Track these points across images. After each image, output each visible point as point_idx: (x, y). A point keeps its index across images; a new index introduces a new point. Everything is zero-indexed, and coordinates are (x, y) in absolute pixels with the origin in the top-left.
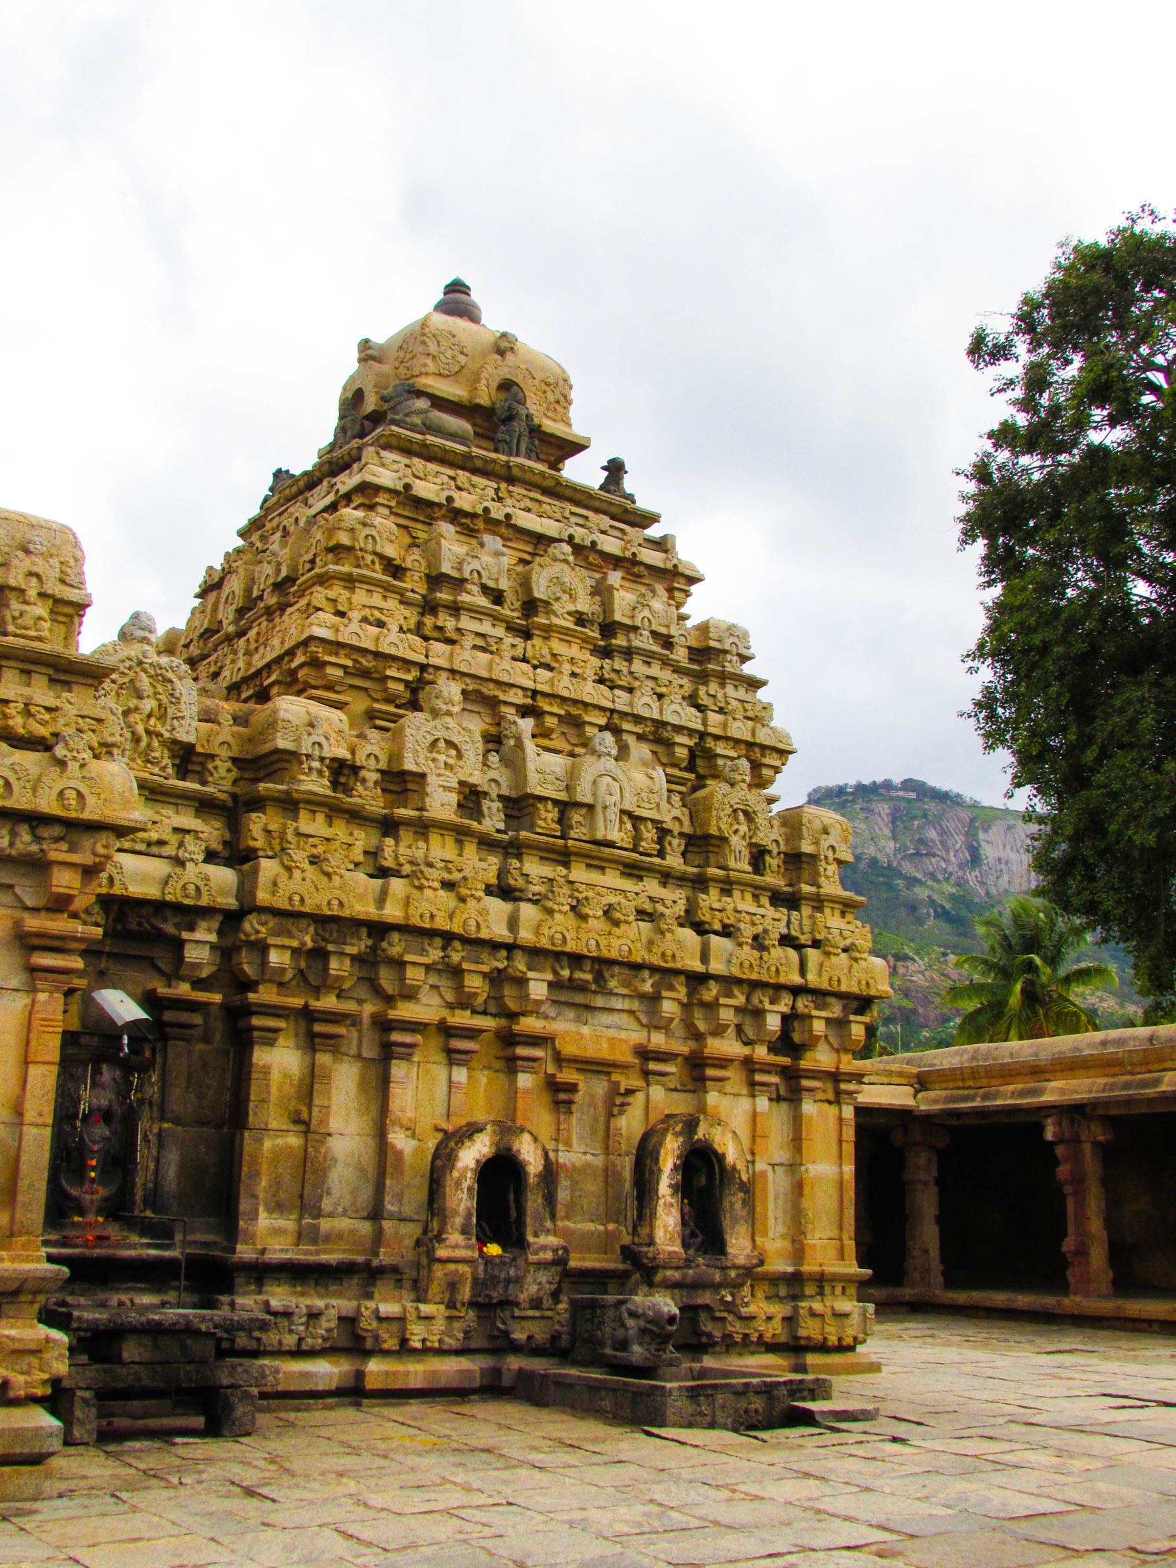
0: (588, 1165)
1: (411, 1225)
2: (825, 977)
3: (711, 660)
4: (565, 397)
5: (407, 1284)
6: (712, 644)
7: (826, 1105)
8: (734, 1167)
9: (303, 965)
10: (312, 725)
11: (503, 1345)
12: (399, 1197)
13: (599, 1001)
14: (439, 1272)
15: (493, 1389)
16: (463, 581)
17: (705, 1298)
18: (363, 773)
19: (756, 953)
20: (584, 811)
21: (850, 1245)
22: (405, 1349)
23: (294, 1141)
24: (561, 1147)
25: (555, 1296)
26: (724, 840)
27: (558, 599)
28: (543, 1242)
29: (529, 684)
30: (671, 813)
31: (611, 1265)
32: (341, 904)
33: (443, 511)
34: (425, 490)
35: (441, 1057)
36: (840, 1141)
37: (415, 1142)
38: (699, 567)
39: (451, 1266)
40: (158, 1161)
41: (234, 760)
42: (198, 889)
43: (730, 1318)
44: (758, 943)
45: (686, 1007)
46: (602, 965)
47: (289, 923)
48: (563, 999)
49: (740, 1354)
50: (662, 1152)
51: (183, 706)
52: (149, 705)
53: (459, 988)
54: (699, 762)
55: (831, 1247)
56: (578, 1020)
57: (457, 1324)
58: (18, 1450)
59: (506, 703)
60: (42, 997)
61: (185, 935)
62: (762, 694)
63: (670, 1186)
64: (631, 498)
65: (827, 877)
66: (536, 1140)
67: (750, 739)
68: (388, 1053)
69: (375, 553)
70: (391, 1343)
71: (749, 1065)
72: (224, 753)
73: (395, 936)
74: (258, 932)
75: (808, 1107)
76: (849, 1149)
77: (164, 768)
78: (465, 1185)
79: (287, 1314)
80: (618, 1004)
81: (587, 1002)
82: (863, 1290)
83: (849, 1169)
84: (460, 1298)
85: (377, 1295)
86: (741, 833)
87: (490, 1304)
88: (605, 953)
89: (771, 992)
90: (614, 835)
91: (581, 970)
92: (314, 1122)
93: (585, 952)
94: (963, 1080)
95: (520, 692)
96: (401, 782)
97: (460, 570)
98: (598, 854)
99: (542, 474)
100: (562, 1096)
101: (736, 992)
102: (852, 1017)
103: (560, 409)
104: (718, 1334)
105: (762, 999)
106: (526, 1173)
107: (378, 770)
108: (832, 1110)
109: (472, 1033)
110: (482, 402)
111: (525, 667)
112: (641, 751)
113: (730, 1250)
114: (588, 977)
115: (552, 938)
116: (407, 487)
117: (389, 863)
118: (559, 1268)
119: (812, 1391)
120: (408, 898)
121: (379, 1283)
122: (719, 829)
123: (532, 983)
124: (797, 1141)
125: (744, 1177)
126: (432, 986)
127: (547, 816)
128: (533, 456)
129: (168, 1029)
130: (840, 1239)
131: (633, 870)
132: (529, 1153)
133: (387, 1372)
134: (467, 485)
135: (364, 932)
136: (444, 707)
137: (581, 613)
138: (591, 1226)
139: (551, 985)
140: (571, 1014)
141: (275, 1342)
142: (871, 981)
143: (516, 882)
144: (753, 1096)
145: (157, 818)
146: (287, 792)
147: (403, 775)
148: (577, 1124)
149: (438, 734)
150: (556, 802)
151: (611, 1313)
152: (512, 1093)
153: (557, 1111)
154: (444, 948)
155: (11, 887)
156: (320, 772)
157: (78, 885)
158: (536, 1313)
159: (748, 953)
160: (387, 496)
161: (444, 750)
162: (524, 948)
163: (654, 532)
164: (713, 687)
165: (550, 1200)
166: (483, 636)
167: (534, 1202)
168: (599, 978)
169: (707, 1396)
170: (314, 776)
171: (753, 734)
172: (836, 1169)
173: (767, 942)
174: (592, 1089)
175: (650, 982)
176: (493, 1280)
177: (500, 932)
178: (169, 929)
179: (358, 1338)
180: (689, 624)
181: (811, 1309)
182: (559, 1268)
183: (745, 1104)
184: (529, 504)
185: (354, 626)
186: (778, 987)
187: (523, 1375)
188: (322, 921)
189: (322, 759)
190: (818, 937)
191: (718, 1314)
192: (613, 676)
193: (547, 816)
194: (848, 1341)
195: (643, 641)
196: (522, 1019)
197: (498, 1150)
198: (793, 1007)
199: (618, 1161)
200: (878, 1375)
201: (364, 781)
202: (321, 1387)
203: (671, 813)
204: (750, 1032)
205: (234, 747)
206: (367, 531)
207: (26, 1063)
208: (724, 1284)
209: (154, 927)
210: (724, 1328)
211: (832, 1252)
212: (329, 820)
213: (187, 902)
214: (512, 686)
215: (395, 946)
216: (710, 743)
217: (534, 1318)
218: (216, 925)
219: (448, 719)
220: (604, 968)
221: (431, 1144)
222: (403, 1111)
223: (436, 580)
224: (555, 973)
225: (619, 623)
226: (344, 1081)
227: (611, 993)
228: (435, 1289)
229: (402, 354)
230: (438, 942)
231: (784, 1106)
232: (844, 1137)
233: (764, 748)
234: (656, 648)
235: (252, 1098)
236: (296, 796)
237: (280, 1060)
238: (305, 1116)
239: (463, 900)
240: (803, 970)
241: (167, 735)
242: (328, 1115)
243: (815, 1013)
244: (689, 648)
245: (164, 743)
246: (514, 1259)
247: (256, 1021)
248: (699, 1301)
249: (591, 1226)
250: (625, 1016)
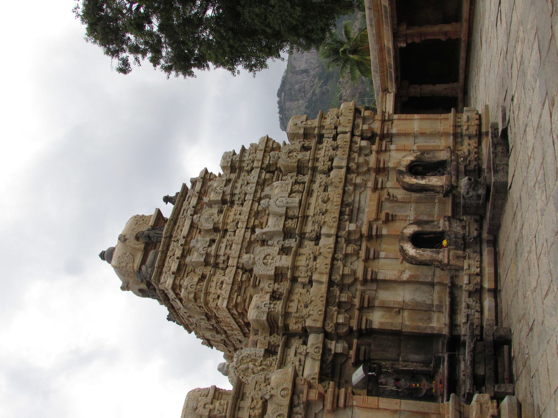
0: (415, 209)
1: (436, 272)
2: (348, 125)
3: (234, 164)
4: (141, 217)
5: (457, 273)
6: (229, 165)
7: (393, 124)
8: (415, 157)
9: (343, 310)
10: (258, 307)
11: (479, 239)
12: (426, 276)
13: (356, 205)
14: (453, 262)
15: (494, 243)
16: (207, 253)
17: (462, 167)
18: (275, 289)
19: (339, 149)
20: (289, 211)
21: (443, 116)
22: (480, 274)
23: (406, 314)
24: (408, 219)
25: (461, 221)
26: (299, 160)
27: (213, 220)
28: (442, 225)
29: (243, 230)
30: (289, 179)
31: (450, 201)
32: (322, 297)
33: (182, 260)
34: (174, 267)
35: (376, 261)
36: (406, 119)
37: (407, 271)
38: (202, 170)
39: (451, 258)
40: (413, 362)
41: (271, 335)
42: (316, 348)
43: (469, 158)
44: (335, 149)
45: (358, 174)
46: (343, 204)
47: (329, 315)
48: (355, 218)
49: (482, 155)
50: (410, 183)
51: (251, 353)
52: (251, 365)
53: (351, 255)
54: (271, 169)
55: (443, 123)
56: (363, 213)
58: (516, 412)
59: (250, 238)
60: (355, 403)
61: (333, 352)
62: (247, 147)
63: (422, 180)
64: (177, 194)
65: (312, 124)
66: (406, 228)
67: (263, 152)
68: (375, 280)
69: (197, 285)
70: (478, 279)
71: (379, 152)
72: (268, 338)
73: (333, 278)
74: (332, 326)
75: (394, 131)
76: (409, 116)
77: (273, 360)
78: (422, 253)
79: (468, 316)
80: (357, 198)
81: (357, 209)
82: (459, 111)
83: (416, 116)
84: (462, 255)
85: (461, 284)
87: (464, 244)
88: (339, 203)
89: (353, 144)
90: (297, 200)
91: (345, 212)
92: (399, 306)
93: (339, 210)
94: (384, 76)
95: (246, 233)
96: (278, 275)
97: (203, 255)
98: (304, 205)
99: (169, 225)
100: (390, 218)
101: (353, 156)
102: (362, 115)
103: (146, 219)
104: (475, 163)
105: (356, 147)
106: (417, 231)
107: (274, 284)
108: (395, 122)
109: (368, 250)
110: (143, 247)
111: (237, 232)
112: (267, 190)
113: (445, 159)
114: (348, 209)
115: (334, 222)
116: (173, 273)
117: (307, 280)
118: (451, 219)
119: (495, 129)
120: (319, 273)
121: (457, 283)
122: (295, 162)
123: (350, 229)
124: (406, 135)
125: (419, 153)
126: (351, 265)
127: (291, 223)
128: (162, 228)
129: (366, 358)
130: (441, 119)
131: (310, 193)
132: (410, 230)
133: (488, 280)
134: (173, 252)
135: (332, 289)
136: (252, 260)
137: (218, 211)
138: (436, 208)
139: (350, 222)
141: (478, 320)
143: (314, 235)
144: (390, 150)
145: (291, 362)
146: (282, 316)
147: (276, 275)
148: (400, 213)
149: (261, 262)
150: (285, 221)
151: (467, 201)
152: (389, 236)
153: (395, 220)
154: (337, 260)
155: (316, 414)
156: (275, 304)
157: (315, 390)
158: (467, 227)
159: (339, 152)
160: (176, 280)
161: (267, 260)
162: (338, 232)
163: (189, 185)
164: (245, 165)
165: (427, 222)
166: (226, 246)
167: (428, 228)
168: (348, 205)
169: (497, 167)
170: (276, 306)
171: (261, 150)
172: (416, 121)
173: (335, 146)
174: (388, 208)
175: (349, 187)
176: (456, 242)
177: (332, 240)
178: (330, 358)
179: (476, 291)
180: (222, 173)
181: (466, 130)
182: (451, 219)
183: (393, 154)
184: (179, 230)
185: (223, 292)
186: (351, 141)
187: (489, 232)
188: (328, 303)
189: (270, 304)
190: (333, 127)
191: (468, 163)
192: (240, 200)
193: (291, 223)
194: (477, 117)
195: (228, 189)
196: (363, 232)
197: (409, 241)
198: (359, 136)
199: (413, 198)
200: (489, 106)
201: (278, 289)
202: (494, 304)
203: (289, 179)
204: (367, 152)
205: (266, 335)
206: (189, 288)
207: (378, 409)
209: (330, 363)
210: (473, 160)
211: (446, 122)
212: (291, 301)
213: (321, 352)
214: (244, 236)
215: (337, 277)
216: (264, 166)
217: (469, 228)
218: (329, 341)
219: (256, 259)
220: (344, 203)
221: (407, 265)
223: (206, 263)
224: (346, 221)
225: (222, 198)
226: (385, 296)
227: (354, 201)
228: (459, 264)
229: (126, 275)
230: (335, 262)
231: (393, 139)
232: (405, 118)
233: (266, 147)
234: (231, 185)
235: (391, 328)
236: (283, 313)
237: (377, 319)
238: (397, 310)
239: (320, 254)
240: (345, 133)
241: (262, 359)
242: (397, 302)
243: (360, 128)
244: (231, 173)
245: (265, 360)
246: (448, 235)
247: (363, 327)
248: (463, 169)
249: (436, 208)
250: (362, 196)
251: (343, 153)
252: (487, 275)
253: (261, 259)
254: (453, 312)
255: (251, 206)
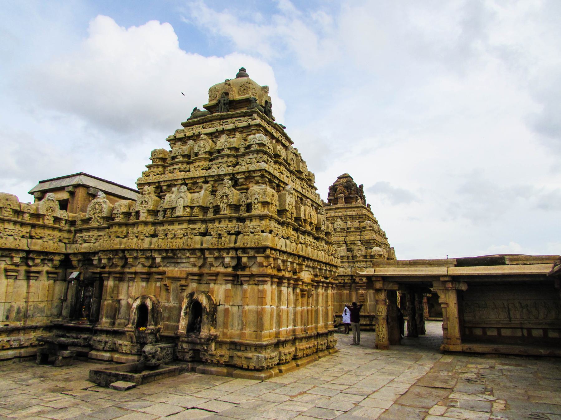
0: (175, 307)
2: (242, 243)
7: (254, 286)
8: (205, 307)
13: (179, 261)
17: (198, 347)
27: (200, 150)
39: (129, 333)
52: (98, 211)
56: (175, 267)
57: (135, 348)
66: (151, 300)
79: (100, 342)
80: (184, 261)
86: (225, 201)
88: (172, 248)
89: (226, 251)
90: (180, 212)
93: (166, 248)
98: (179, 220)
99: (215, 116)
101: (215, 253)
104: (204, 359)
108: (256, 287)
112: (184, 188)
113: (201, 333)
131: (191, 222)
132: (149, 303)
135: (120, 252)
140: (173, 265)
142: (259, 242)
162: (155, 250)
171: (248, 168)
177: (146, 246)
184: (210, 126)
186: (228, 250)
195: (226, 152)
208: (201, 344)
222: (131, 293)
227: (181, 258)
233: (254, 171)
237: (110, 283)
240: (236, 242)
250: (188, 264)
251: (213, 244)
252: (121, 357)
253: (144, 199)
254: (107, 332)
255: (200, 177)
